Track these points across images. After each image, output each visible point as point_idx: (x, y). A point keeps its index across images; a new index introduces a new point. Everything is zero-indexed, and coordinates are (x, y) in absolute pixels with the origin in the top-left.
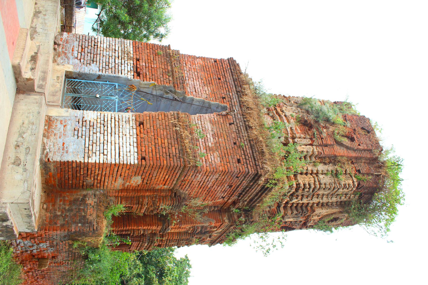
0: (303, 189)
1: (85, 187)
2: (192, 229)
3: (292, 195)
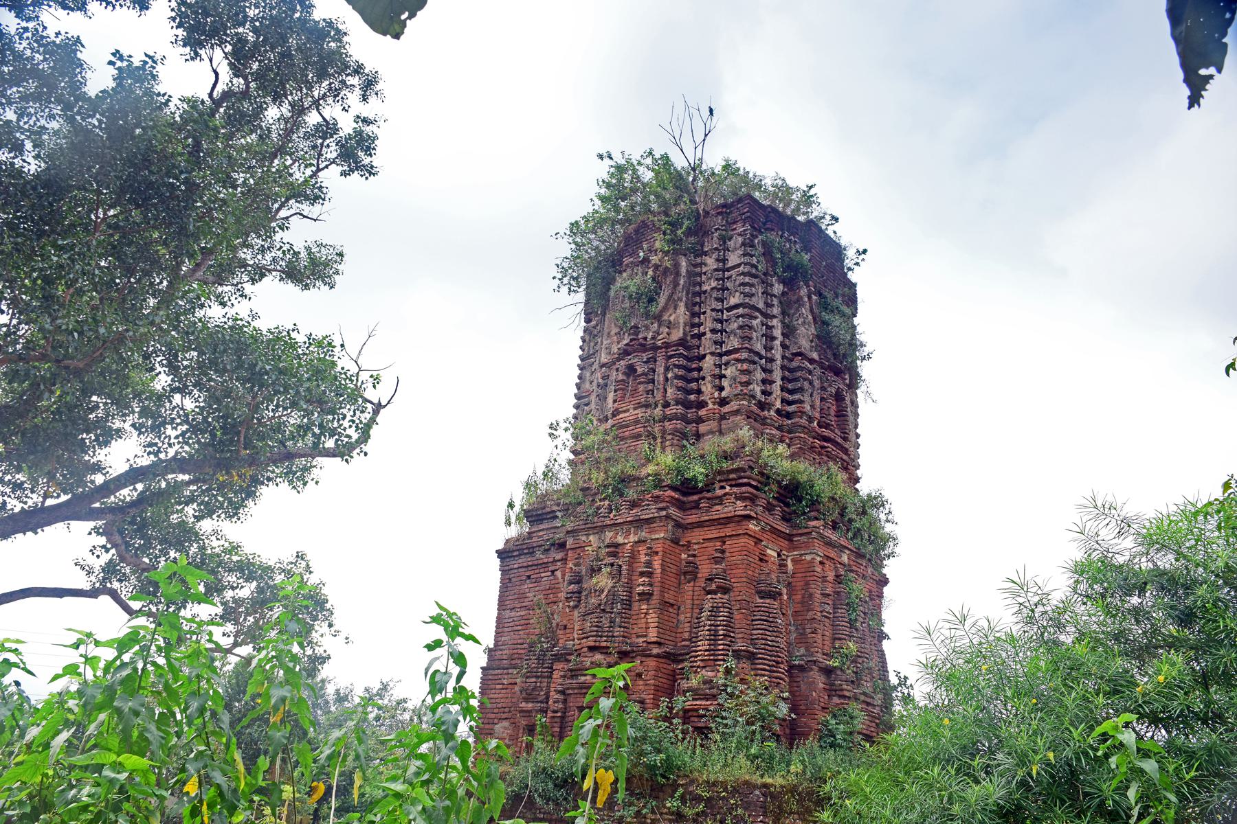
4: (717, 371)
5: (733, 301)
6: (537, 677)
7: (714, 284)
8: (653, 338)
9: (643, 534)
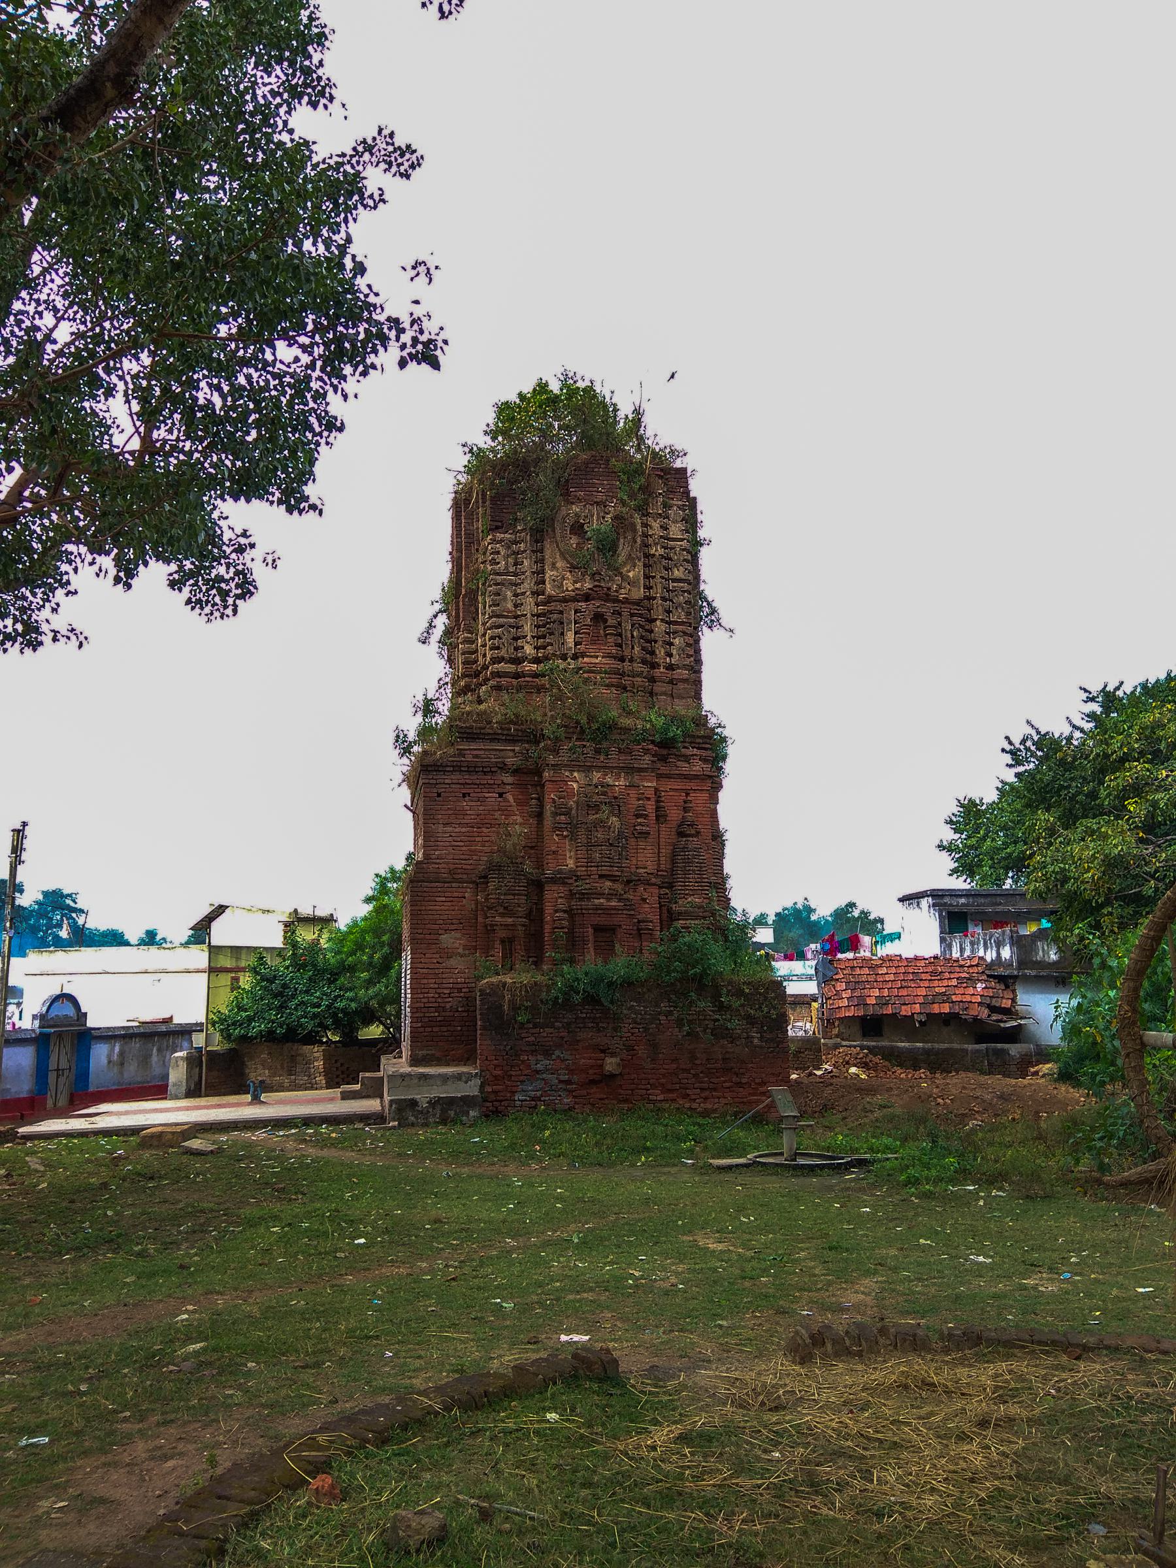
0: (498, 648)
3: (517, 661)
4: (667, 638)
5: (677, 573)
6: (514, 895)
7: (661, 551)
8: (616, 591)
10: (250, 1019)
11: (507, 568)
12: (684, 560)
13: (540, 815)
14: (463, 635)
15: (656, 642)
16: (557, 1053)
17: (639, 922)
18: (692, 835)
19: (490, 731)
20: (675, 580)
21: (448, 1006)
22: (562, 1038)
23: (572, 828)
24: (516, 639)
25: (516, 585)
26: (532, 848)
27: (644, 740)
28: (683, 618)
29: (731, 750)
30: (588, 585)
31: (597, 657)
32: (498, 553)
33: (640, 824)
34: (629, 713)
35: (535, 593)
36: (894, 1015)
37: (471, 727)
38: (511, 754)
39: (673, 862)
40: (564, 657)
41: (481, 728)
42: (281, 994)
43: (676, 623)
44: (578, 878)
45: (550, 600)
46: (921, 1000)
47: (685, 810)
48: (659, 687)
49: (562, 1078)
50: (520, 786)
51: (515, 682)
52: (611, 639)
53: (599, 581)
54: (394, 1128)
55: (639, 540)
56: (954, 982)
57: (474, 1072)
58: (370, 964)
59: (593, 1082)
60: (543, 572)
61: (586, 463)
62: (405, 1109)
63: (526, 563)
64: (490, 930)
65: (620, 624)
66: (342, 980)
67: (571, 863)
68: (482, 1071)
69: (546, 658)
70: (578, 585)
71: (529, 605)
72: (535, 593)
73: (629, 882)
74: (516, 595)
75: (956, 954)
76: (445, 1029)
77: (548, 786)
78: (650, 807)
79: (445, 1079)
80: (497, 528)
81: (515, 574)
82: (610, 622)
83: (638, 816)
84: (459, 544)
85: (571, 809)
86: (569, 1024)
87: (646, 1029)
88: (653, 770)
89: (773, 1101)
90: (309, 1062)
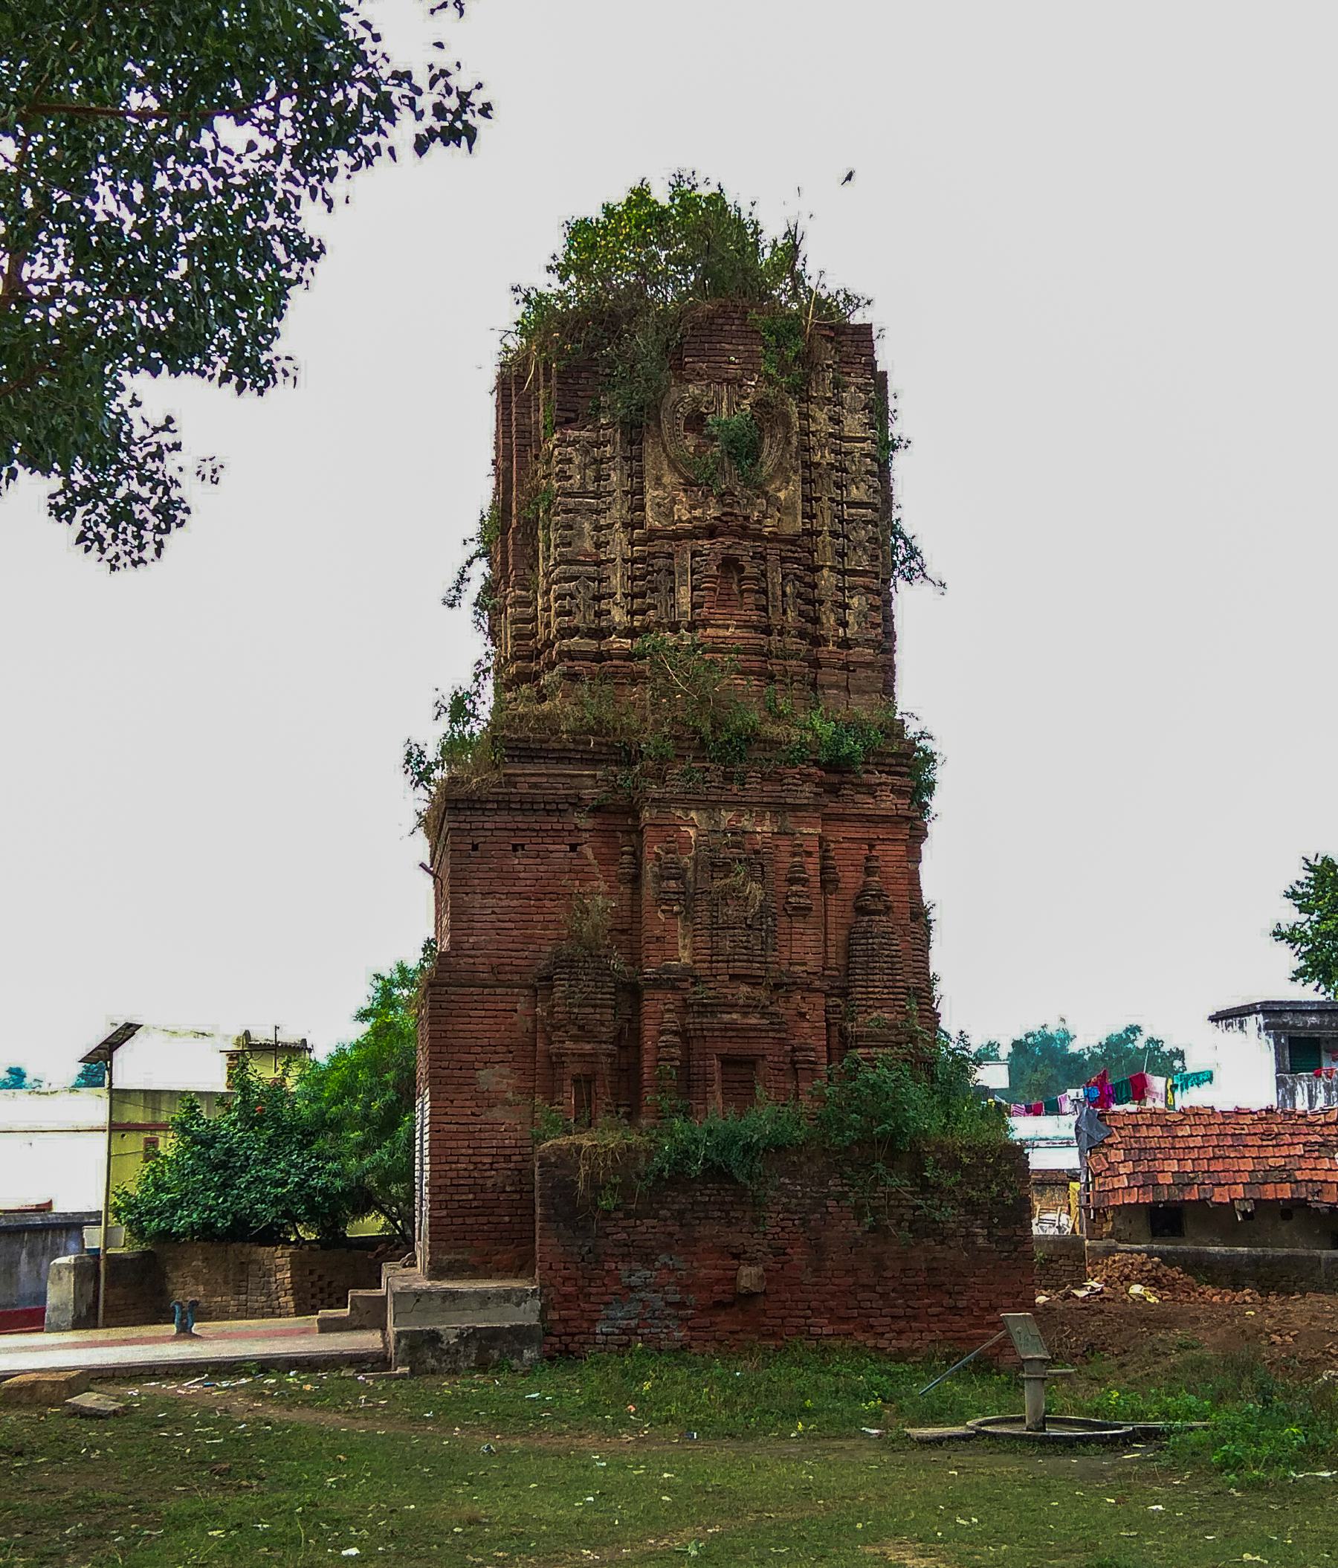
0: (569, 613)
1: (527, 1188)
2: (664, 907)
6: (595, 1006)
7: (830, 458)
8: (759, 522)
9: (790, 823)
10: (175, 1205)
11: (583, 485)
12: (868, 472)
13: (635, 880)
14: (514, 593)
15: (821, 603)
16: (663, 1258)
17: (794, 1050)
18: (878, 913)
19: (557, 746)
20: (853, 504)
21: (489, 1183)
22: (671, 1235)
23: (688, 899)
24: (598, 598)
25: (598, 512)
26: (623, 931)
27: (803, 760)
28: (865, 564)
29: (940, 774)
30: (713, 513)
31: (727, 627)
32: (570, 461)
33: (795, 894)
34: (779, 717)
35: (629, 526)
36: (1202, 1202)
37: (527, 740)
38: (590, 782)
39: (849, 955)
40: (674, 628)
41: (542, 741)
42: (223, 1165)
43: (854, 573)
44: (697, 980)
45: (653, 535)
46: (1246, 1178)
47: (869, 871)
48: (825, 676)
49: (671, 1298)
50: (605, 833)
51: (596, 667)
52: (750, 599)
53: (731, 505)
54: (403, 1376)
55: (794, 440)
56: (1299, 1150)
57: (531, 1288)
58: (366, 1117)
59: (719, 1305)
60: (641, 491)
61: (711, 318)
62: (420, 1346)
63: (614, 477)
64: (555, 1062)
65: (764, 574)
66: (319, 1144)
67: (685, 956)
68: (543, 1287)
69: (646, 629)
70: (697, 513)
71: (619, 545)
72: (629, 526)
73: (777, 986)
74: (598, 528)
75: (1301, 1104)
76: (483, 1220)
77: (649, 833)
78: (813, 865)
79: (484, 1299)
80: (568, 421)
81: (597, 496)
82: (750, 570)
83: (792, 881)
84: (507, 447)
85: (685, 870)
86: (681, 1213)
87: (805, 1222)
88: (816, 807)
89: (1008, 1337)
90: (268, 1273)
